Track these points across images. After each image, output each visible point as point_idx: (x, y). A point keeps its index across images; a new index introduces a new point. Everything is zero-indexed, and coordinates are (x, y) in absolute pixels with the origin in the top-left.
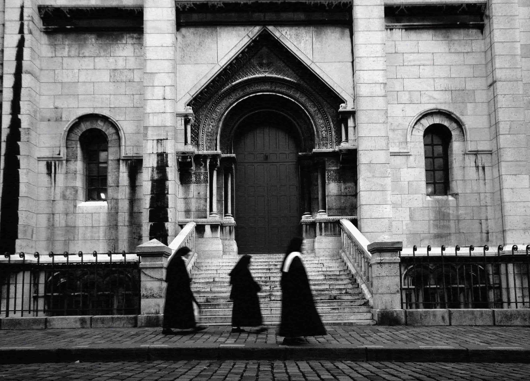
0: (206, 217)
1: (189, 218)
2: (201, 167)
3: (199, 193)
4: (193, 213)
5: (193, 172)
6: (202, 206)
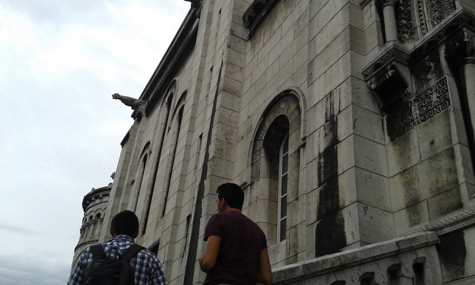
0: (460, 206)
1: (418, 223)
2: (429, 76)
3: (432, 143)
4: (424, 205)
5: (412, 100)
6: (444, 176)
